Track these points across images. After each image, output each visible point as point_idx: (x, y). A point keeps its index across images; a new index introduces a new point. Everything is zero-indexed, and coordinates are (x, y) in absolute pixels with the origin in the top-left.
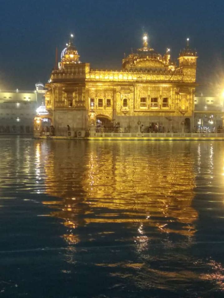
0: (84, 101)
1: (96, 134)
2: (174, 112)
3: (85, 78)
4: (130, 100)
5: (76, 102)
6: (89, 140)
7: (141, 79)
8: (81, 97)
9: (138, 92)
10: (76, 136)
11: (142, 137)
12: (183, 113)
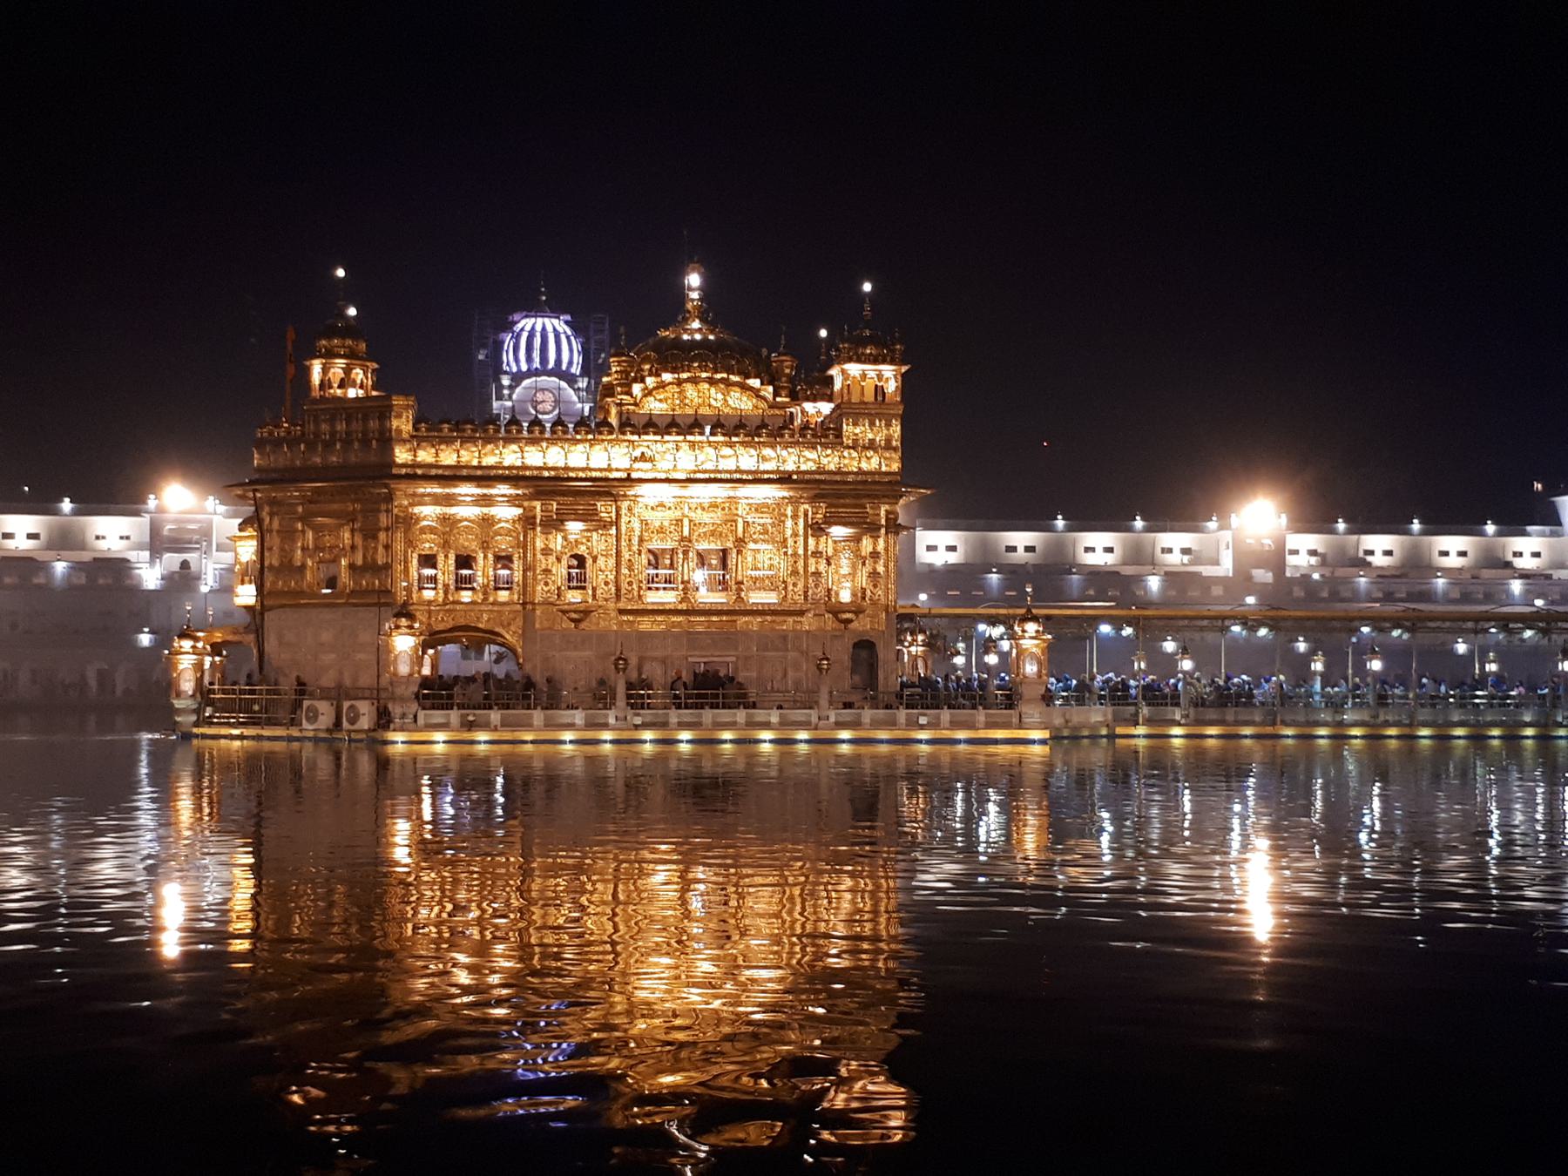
0: (387, 567)
1: (421, 714)
2: (801, 613)
3: (393, 464)
4: (601, 561)
5: (352, 567)
6: (386, 743)
8: (376, 549)
9: (636, 525)
10: (338, 724)
11: (636, 727)
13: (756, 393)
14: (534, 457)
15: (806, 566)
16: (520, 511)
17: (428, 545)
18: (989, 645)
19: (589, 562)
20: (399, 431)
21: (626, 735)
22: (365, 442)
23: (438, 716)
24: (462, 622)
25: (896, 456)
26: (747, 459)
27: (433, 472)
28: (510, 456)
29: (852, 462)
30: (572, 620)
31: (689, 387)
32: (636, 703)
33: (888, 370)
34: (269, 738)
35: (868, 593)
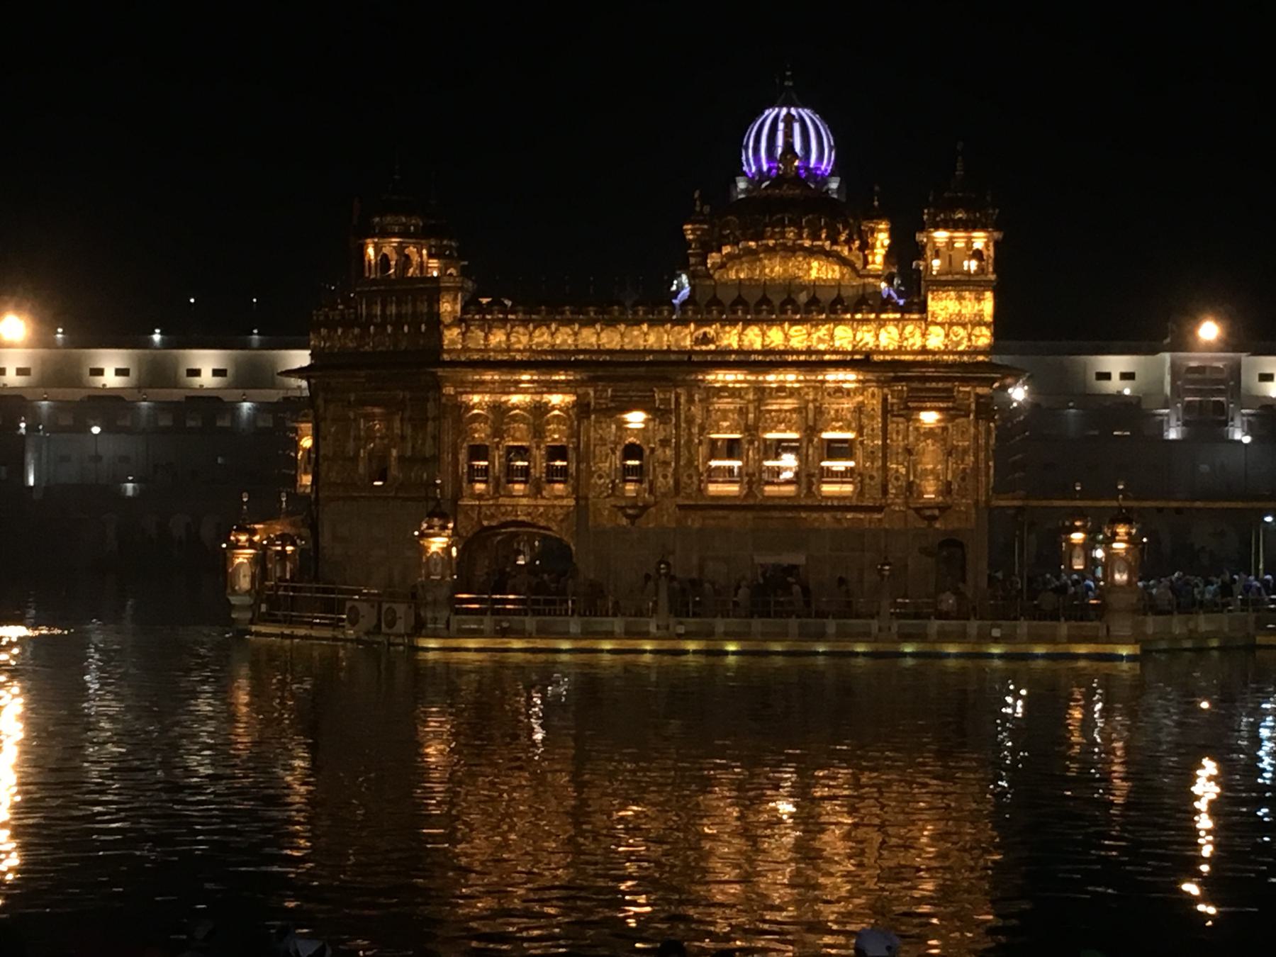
0: (436, 459)
2: (879, 509)
3: (439, 349)
4: (659, 452)
5: (401, 458)
7: (712, 347)
8: (424, 440)
11: (680, 637)
12: (928, 513)
13: (843, 261)
16: (570, 399)
19: (647, 452)
21: (667, 645)
29: (936, 339)
30: (628, 516)
32: (680, 609)
35: (955, 486)
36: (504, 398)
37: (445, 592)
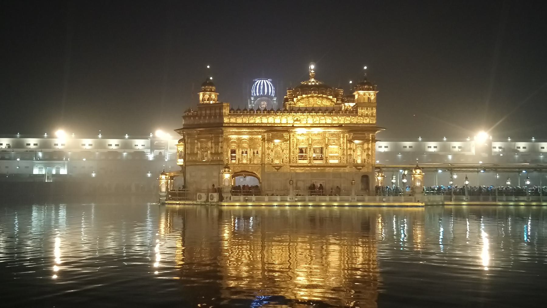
0: (222, 153)
1: (232, 197)
2: (346, 167)
3: (223, 123)
4: (285, 151)
5: (211, 153)
6: (222, 206)
9: (295, 140)
11: (296, 201)
14: (265, 120)
15: (347, 152)
17: (234, 146)
18: (404, 176)
20: (225, 113)
22: (215, 116)
23: (237, 198)
24: (244, 170)
25: (375, 119)
26: (329, 120)
27: (235, 125)
28: (257, 120)
31: (311, 98)
33: (372, 93)
34: (187, 204)
36: (241, 136)
37: (230, 189)
